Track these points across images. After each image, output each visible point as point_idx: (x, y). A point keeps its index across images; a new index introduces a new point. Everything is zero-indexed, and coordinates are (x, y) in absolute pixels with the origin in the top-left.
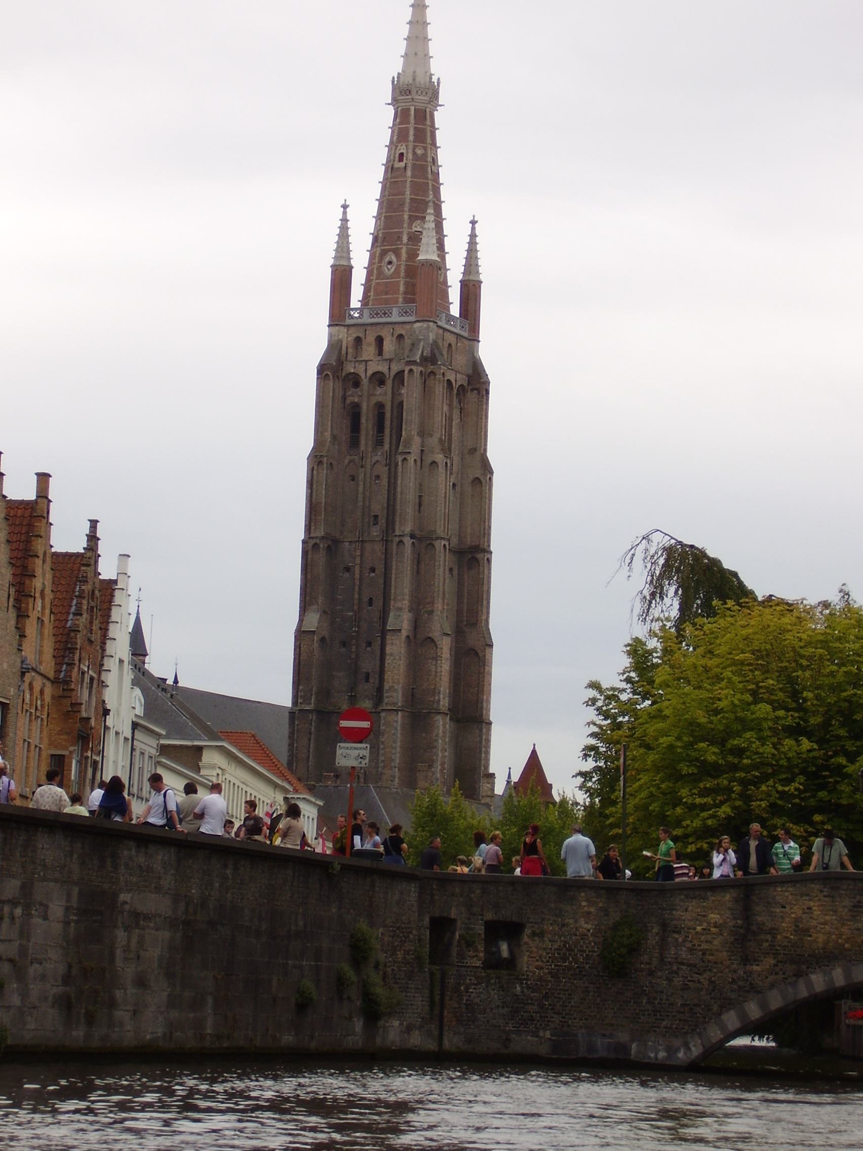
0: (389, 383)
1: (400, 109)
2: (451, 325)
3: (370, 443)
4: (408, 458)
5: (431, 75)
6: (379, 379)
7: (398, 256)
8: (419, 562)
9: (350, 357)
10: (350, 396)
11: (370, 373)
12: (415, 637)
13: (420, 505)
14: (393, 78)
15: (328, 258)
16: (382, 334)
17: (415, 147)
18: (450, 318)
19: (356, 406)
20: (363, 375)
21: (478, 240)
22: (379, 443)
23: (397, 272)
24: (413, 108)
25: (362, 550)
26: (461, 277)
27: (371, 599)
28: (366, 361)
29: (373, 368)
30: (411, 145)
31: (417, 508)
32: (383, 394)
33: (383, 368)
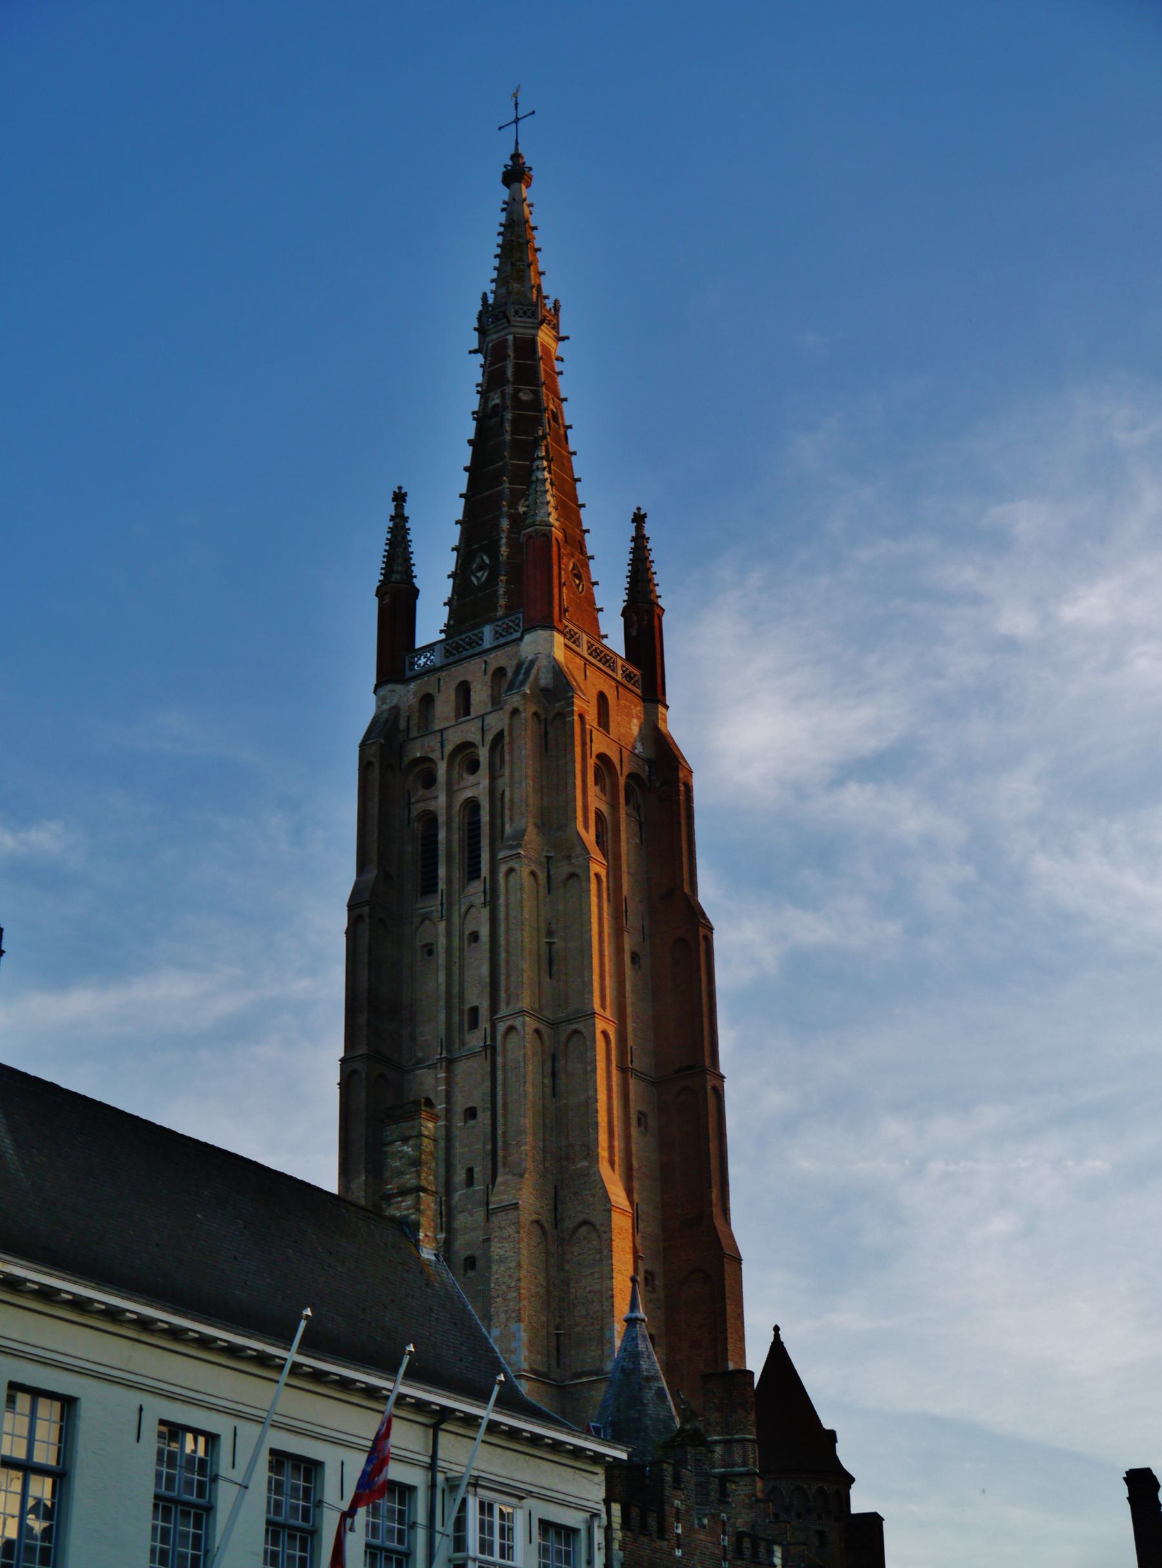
0: (483, 754)
1: (491, 345)
3: (456, 874)
4: (517, 867)
5: (542, 297)
6: (465, 756)
7: (494, 553)
8: (554, 1075)
9: (414, 733)
10: (418, 802)
11: (449, 748)
12: (557, 1222)
13: (551, 962)
16: (469, 678)
17: (517, 391)
19: (430, 820)
20: (436, 755)
22: (473, 872)
24: (510, 337)
25: (449, 1082)
27: (470, 1171)
28: (442, 731)
29: (454, 738)
30: (509, 389)
31: (545, 965)
32: (477, 787)
33: (470, 731)
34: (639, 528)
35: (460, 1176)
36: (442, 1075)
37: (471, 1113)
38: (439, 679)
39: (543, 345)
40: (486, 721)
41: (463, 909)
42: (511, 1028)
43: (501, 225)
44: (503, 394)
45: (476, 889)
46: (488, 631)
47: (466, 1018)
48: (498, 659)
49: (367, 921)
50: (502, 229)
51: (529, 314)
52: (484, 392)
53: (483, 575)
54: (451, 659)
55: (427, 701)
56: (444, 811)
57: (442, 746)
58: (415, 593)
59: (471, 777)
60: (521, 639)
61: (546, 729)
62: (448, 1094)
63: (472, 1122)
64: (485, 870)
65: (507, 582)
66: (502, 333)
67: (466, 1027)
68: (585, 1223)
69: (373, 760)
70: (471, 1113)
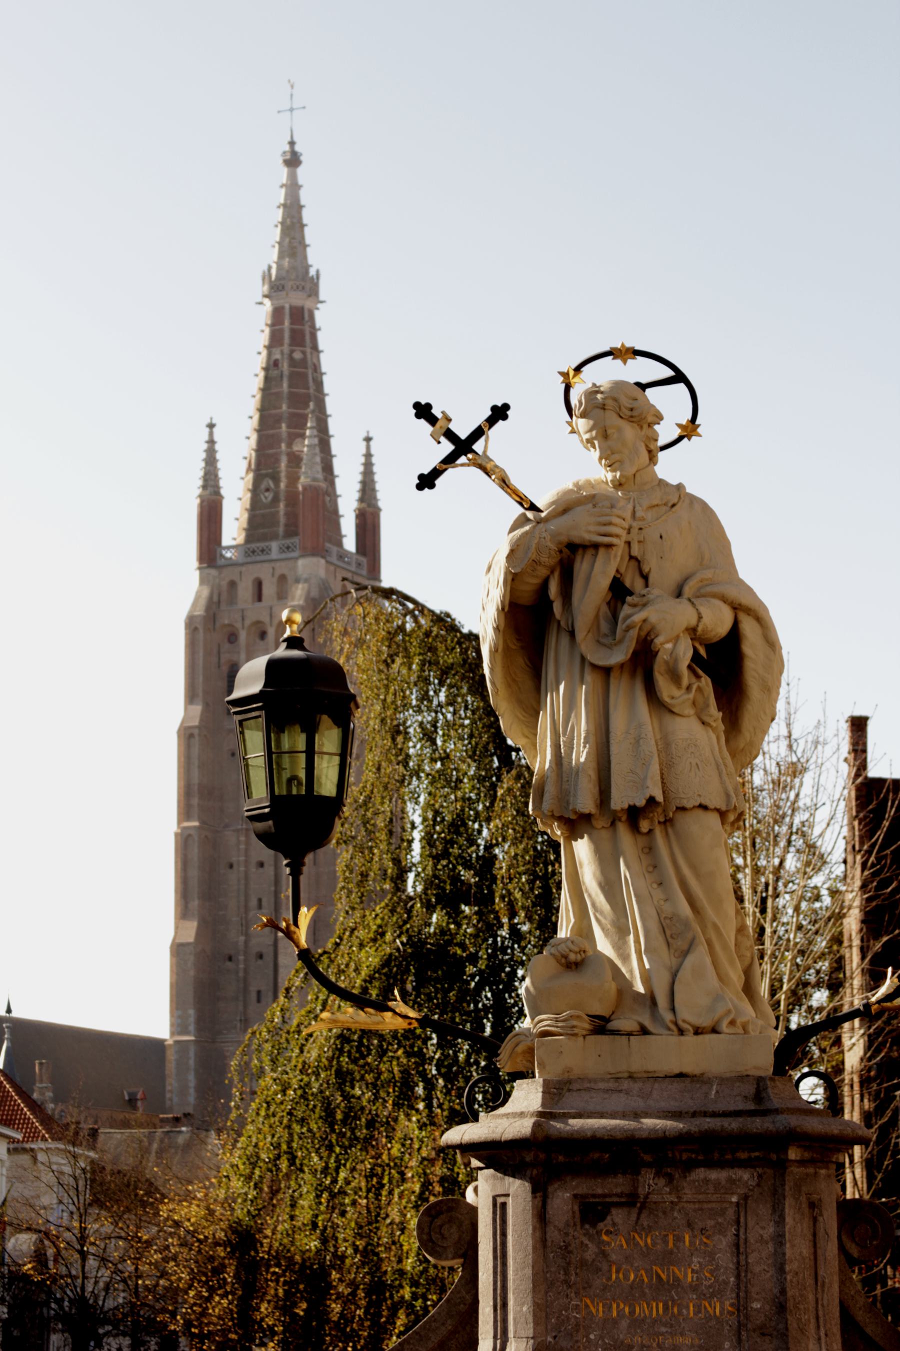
2: (344, 562)
11: (248, 622)
14: (264, 273)
17: (292, 352)
18: (343, 555)
20: (238, 625)
21: (374, 460)
23: (276, 500)
24: (287, 306)
26: (355, 505)
27: (260, 900)
30: (286, 348)
35: (254, 902)
36: (243, 839)
37: (261, 865)
38: (241, 573)
44: (282, 353)
46: (274, 545)
48: (281, 568)
52: (269, 348)
53: (270, 496)
54: (249, 559)
55: (233, 584)
57: (243, 619)
59: (262, 643)
60: (297, 559)
63: (261, 870)
65: (287, 506)
70: (261, 865)
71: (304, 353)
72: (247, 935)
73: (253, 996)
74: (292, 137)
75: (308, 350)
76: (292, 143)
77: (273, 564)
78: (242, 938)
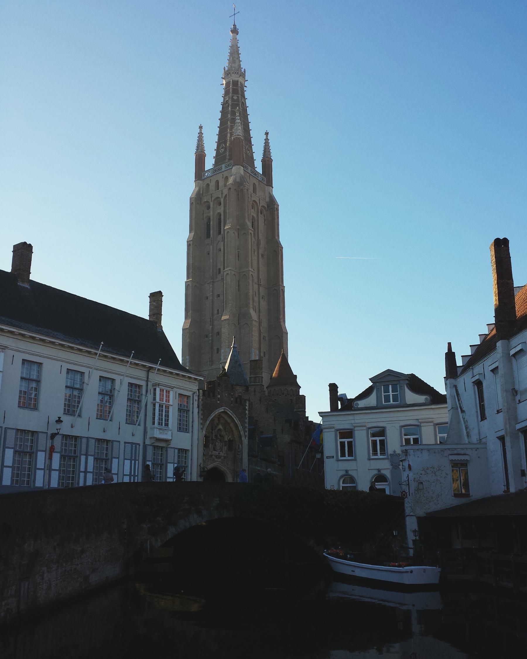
0: (222, 200)
8: (239, 286)
15: (194, 150)
17: (233, 96)
20: (210, 201)
24: (231, 80)
27: (218, 310)
32: (221, 209)
34: (267, 136)
35: (216, 312)
39: (240, 82)
40: (223, 191)
41: (217, 243)
42: (228, 274)
43: (230, 46)
45: (220, 236)
46: (223, 166)
47: (218, 271)
49: (192, 245)
50: (230, 48)
51: (237, 73)
55: (208, 185)
56: (212, 216)
58: (204, 156)
60: (232, 168)
61: (238, 193)
62: (213, 291)
64: (222, 232)
66: (229, 79)
67: (217, 273)
68: (246, 323)
69: (193, 202)
70: (218, 296)
71: (238, 97)
72: (213, 325)
73: (216, 350)
74: (234, 23)
75: (240, 96)
76: (234, 25)
77: (222, 173)
78: (211, 327)
